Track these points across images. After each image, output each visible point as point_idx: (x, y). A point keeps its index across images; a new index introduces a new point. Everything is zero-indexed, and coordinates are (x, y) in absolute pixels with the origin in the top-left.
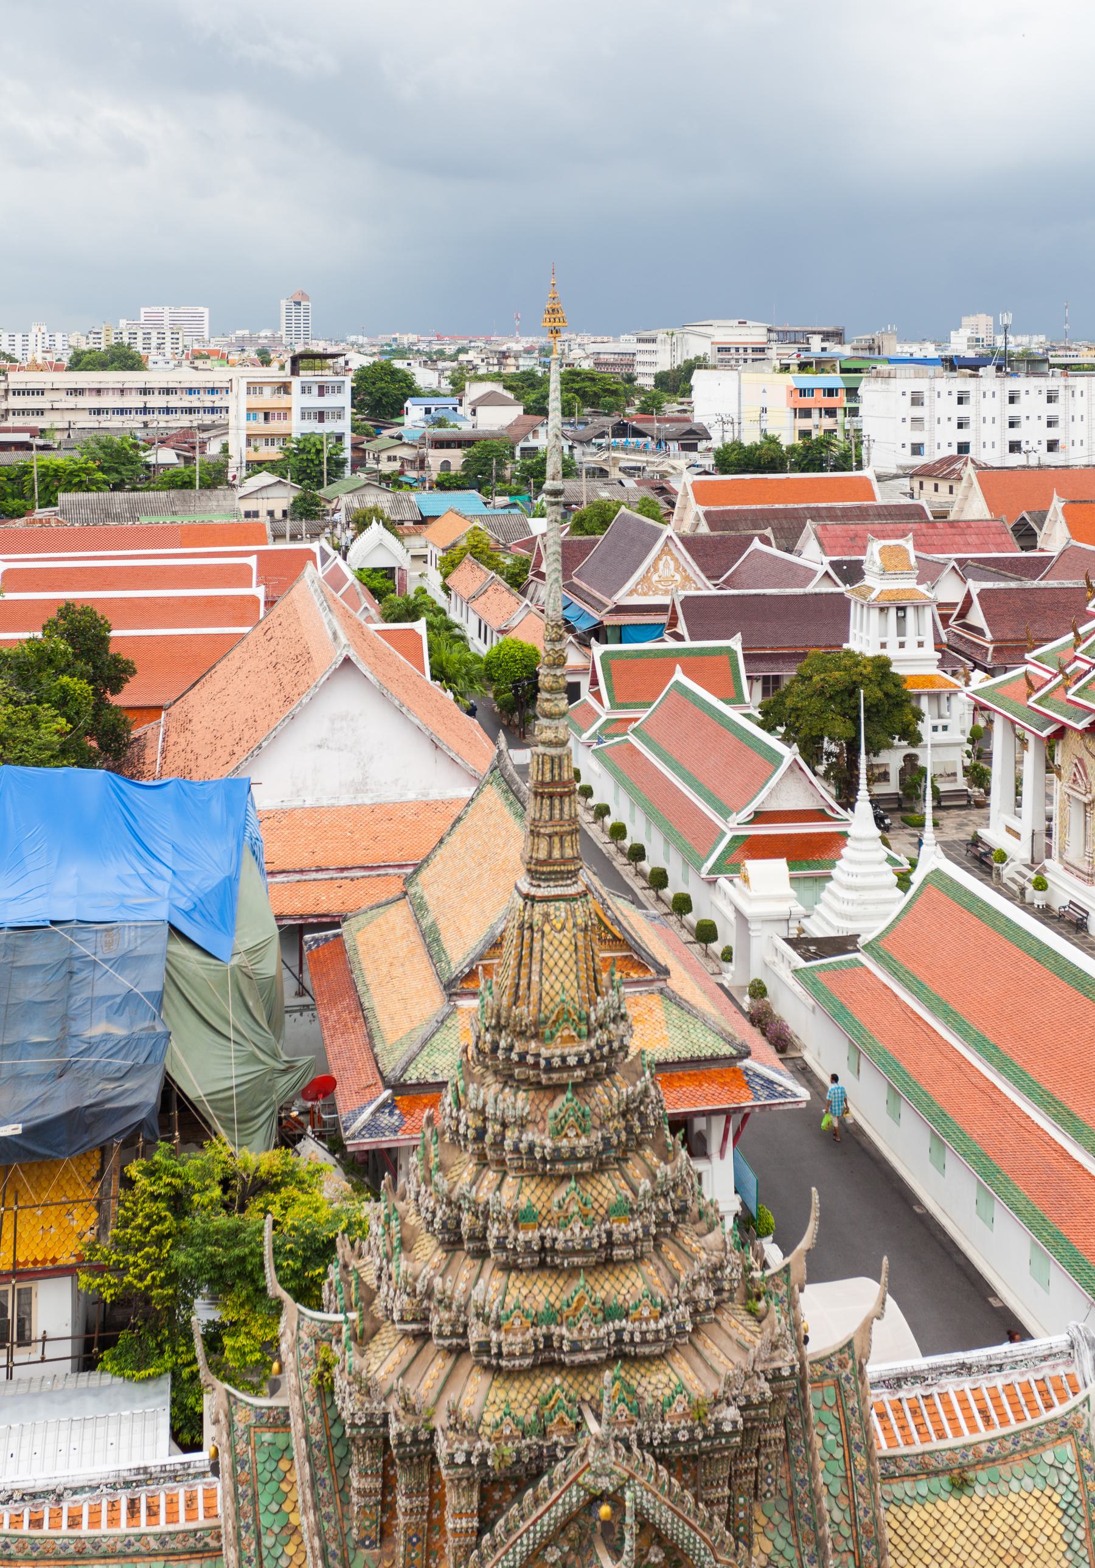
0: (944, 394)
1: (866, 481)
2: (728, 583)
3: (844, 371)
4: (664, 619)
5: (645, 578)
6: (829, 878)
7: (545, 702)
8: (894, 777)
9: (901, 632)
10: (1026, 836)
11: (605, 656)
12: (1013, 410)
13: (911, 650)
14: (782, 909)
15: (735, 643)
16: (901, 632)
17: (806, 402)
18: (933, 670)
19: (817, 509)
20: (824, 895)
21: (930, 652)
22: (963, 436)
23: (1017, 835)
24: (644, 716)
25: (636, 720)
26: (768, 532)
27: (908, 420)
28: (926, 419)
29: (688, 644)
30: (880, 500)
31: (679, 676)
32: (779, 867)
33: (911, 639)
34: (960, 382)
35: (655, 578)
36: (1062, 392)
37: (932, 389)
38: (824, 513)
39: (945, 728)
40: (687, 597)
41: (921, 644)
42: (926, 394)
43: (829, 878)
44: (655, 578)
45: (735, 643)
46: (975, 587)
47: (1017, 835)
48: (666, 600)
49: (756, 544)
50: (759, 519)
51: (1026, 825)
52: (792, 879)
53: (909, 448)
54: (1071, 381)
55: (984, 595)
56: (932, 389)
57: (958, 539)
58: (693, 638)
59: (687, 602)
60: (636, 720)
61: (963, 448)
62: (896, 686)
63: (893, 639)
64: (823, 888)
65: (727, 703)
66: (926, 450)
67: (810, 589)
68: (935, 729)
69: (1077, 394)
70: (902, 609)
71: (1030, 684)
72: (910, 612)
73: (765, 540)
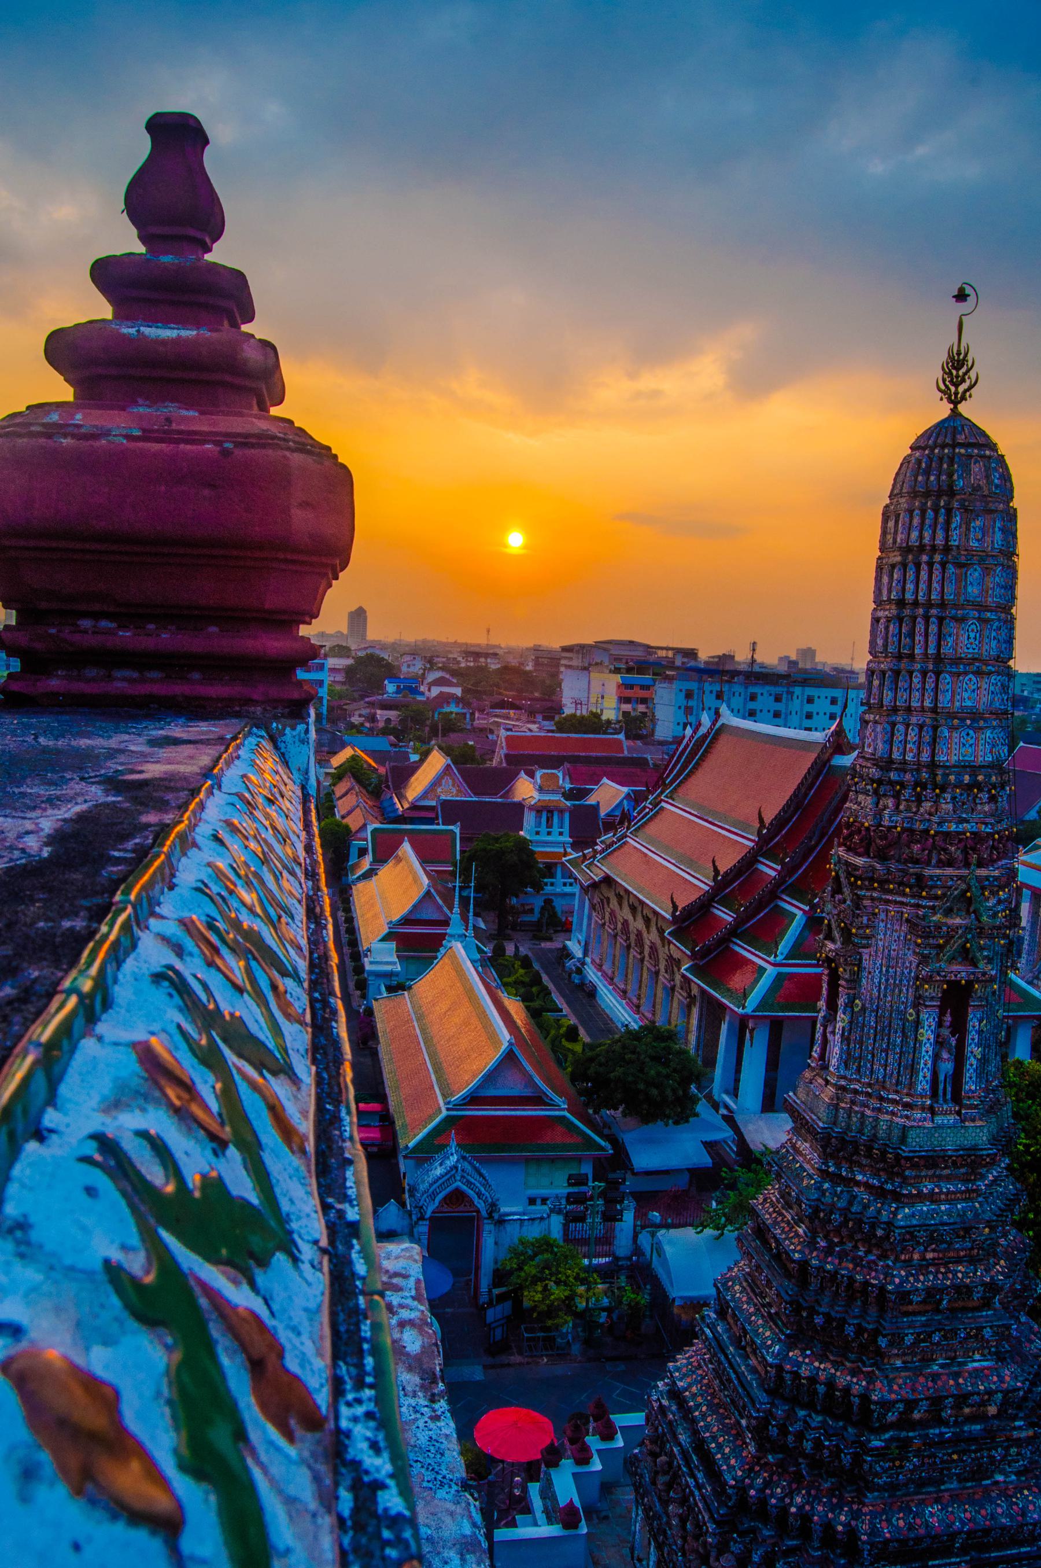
1: (620, 742)
4: (432, 815)
8: (537, 910)
11: (375, 831)
15: (456, 829)
17: (629, 693)
29: (441, 827)
33: (555, 830)
35: (439, 790)
41: (561, 834)
44: (439, 790)
45: (456, 829)
48: (433, 803)
51: (582, 938)
63: (543, 829)
68: (565, 884)
70: (550, 812)
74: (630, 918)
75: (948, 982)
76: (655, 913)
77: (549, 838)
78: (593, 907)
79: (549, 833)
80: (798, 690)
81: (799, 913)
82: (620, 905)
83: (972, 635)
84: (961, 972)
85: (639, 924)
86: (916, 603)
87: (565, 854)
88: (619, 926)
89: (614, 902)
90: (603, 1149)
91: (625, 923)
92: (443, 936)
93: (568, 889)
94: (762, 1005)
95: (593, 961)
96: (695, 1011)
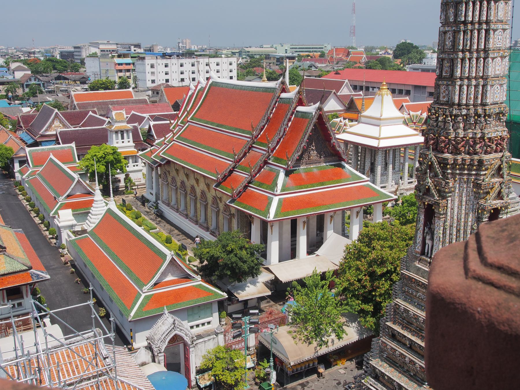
0: (161, 64)
2: (83, 126)
3: (132, 57)
5: (50, 126)
6: (89, 212)
7: (17, 167)
9: (123, 138)
10: (154, 194)
12: (182, 69)
13: (126, 144)
14: (70, 223)
15: (73, 145)
16: (123, 138)
18: (133, 149)
19: (113, 101)
20: (88, 217)
21: (132, 144)
22: (167, 77)
23: (152, 194)
24: (41, 169)
25: (38, 171)
26: (95, 109)
27: (150, 73)
28: (156, 72)
30: (134, 98)
31: (52, 156)
32: (69, 211)
34: (165, 61)
36: (196, 64)
37: (157, 63)
38: (115, 103)
39: (137, 165)
40: (61, 131)
41: (129, 142)
42: (155, 65)
43: (89, 212)
45: (73, 145)
46: (152, 123)
47: (152, 194)
48: (55, 133)
49: (90, 113)
50: (93, 105)
51: (154, 192)
52: (73, 215)
53: (150, 81)
54: (198, 60)
55: (154, 126)
56: (157, 63)
57: (155, 109)
58: (63, 144)
59: (61, 133)
60: (38, 171)
61: (167, 81)
62: (118, 155)
63: (120, 140)
64: (88, 216)
65: (63, 164)
66: (156, 81)
67: (104, 126)
68: (134, 166)
69: (200, 63)
70: (122, 132)
71: (152, 152)
72: (125, 132)
73: (94, 112)
74: (185, 180)
75: (494, 209)
76: (204, 176)
77: (123, 145)
78: (159, 176)
79: (123, 142)
80: (201, 60)
81: (282, 170)
82: (178, 174)
83: (500, 37)
84: (498, 203)
85: (193, 182)
86: (472, 23)
87: (138, 152)
88: (179, 184)
89: (173, 173)
90: (223, 296)
91: (183, 183)
92: (92, 201)
93: (136, 168)
94: (276, 215)
95: (163, 202)
96: (235, 222)
